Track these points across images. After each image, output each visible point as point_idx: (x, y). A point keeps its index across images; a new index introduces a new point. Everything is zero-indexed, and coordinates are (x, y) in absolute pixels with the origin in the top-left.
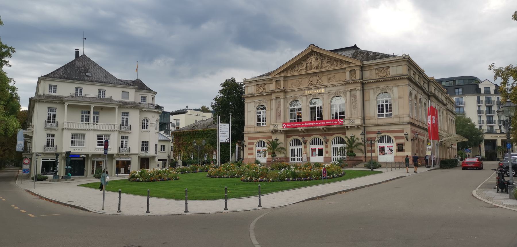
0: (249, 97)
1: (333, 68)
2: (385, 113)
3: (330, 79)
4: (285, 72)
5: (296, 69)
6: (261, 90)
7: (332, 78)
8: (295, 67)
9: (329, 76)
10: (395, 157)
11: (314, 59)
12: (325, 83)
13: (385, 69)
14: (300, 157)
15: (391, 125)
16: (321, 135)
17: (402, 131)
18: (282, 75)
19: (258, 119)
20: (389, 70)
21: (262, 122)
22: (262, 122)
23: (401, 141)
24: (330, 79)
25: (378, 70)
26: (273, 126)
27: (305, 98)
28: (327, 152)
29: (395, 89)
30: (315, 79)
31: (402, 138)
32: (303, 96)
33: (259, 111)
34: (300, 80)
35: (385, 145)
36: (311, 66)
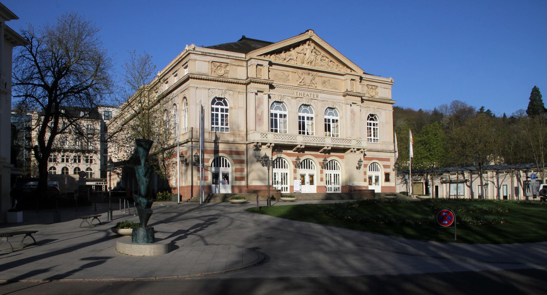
0: (201, 79)
1: (329, 70)
2: (372, 137)
3: (324, 83)
4: (269, 56)
5: (283, 55)
6: (221, 72)
7: (327, 84)
8: (281, 53)
9: (324, 79)
10: (382, 187)
11: (308, 52)
12: (320, 87)
13: (374, 87)
14: (286, 186)
15: (382, 151)
16: (316, 156)
17: (388, 160)
18: (267, 58)
19: (212, 119)
20: (377, 90)
21: (220, 126)
22: (220, 126)
23: (388, 171)
24: (324, 83)
25: (368, 88)
26: (259, 135)
27: (294, 101)
28: (322, 180)
29: (383, 112)
30: (308, 78)
31: (388, 167)
32: (292, 98)
33: (215, 106)
34: (286, 73)
35: (373, 174)
36: (303, 59)
